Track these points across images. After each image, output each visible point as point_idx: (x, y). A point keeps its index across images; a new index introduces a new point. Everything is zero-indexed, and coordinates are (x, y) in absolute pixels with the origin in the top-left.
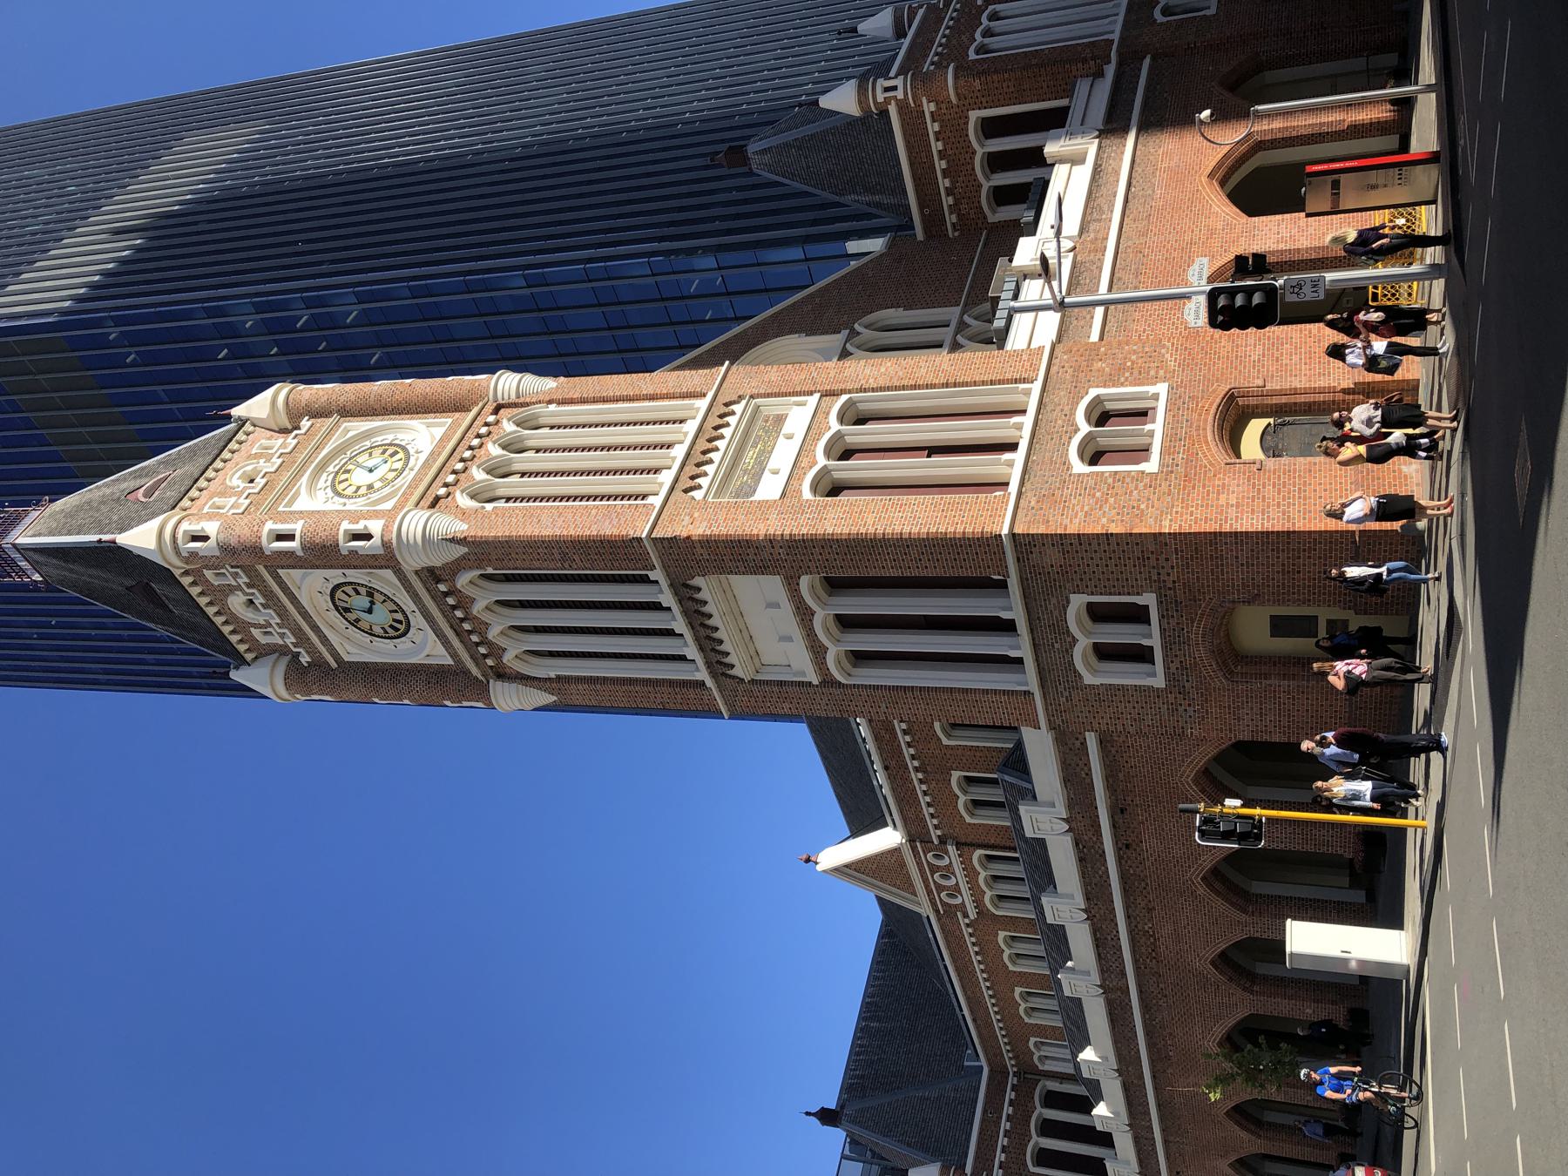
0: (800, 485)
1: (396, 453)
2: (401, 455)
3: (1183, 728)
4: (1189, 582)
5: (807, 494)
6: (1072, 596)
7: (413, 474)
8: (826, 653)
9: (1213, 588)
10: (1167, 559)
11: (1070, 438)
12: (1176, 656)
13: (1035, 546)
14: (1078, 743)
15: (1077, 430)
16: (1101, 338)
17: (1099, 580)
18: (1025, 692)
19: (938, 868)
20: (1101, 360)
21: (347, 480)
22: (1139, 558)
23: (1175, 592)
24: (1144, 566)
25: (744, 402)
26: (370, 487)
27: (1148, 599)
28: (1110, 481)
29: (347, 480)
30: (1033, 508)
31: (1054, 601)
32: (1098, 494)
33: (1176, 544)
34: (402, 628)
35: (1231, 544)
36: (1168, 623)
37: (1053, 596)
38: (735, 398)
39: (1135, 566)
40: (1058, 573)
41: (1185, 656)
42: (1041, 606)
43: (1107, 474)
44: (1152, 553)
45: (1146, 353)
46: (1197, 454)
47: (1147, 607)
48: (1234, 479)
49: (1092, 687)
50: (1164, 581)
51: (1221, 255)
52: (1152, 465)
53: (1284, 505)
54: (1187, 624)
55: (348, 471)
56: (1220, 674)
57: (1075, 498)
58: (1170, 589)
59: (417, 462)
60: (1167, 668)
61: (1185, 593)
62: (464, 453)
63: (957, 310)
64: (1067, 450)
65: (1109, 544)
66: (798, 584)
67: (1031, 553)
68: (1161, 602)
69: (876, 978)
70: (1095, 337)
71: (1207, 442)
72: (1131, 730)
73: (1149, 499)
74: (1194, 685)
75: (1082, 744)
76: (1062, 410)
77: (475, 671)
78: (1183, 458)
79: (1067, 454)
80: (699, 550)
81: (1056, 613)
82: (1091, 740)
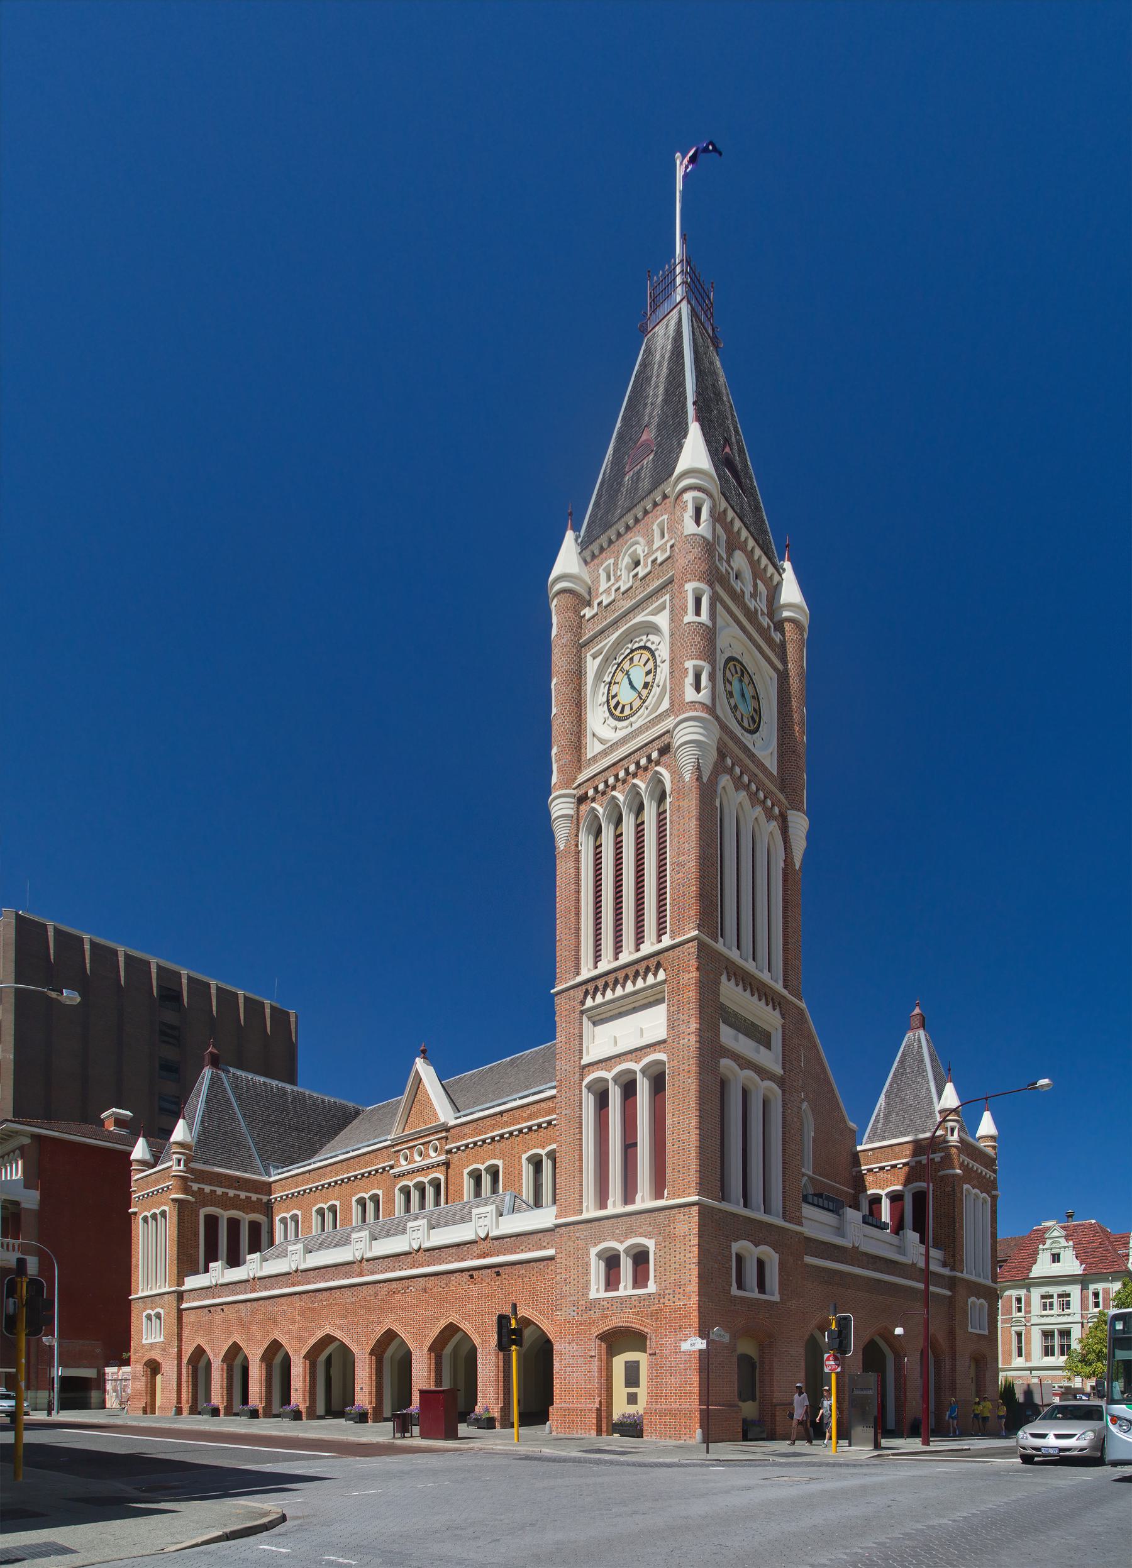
3: (561, 1310)
4: (664, 1312)
8: (607, 1071)
9: (659, 1327)
10: (679, 1299)
12: (612, 1305)
13: (689, 1217)
14: (545, 1244)
17: (665, 1258)
18: (582, 1210)
22: (680, 1282)
23: (657, 1304)
24: (675, 1286)
27: (652, 1287)
30: (712, 1217)
31: (650, 1229)
33: (690, 1304)
36: (635, 1300)
39: (675, 1280)
40: (670, 1232)
41: (612, 1310)
44: (684, 1290)
47: (646, 1286)
49: (588, 1254)
50: (664, 1298)
54: (635, 1312)
56: (601, 1331)
57: (718, 1243)
58: (659, 1301)
60: (604, 1299)
61: (656, 1310)
65: (690, 1264)
66: (659, 1052)
67: (684, 1215)
68: (650, 1296)
72: (558, 1277)
75: (545, 1247)
77: (582, 778)
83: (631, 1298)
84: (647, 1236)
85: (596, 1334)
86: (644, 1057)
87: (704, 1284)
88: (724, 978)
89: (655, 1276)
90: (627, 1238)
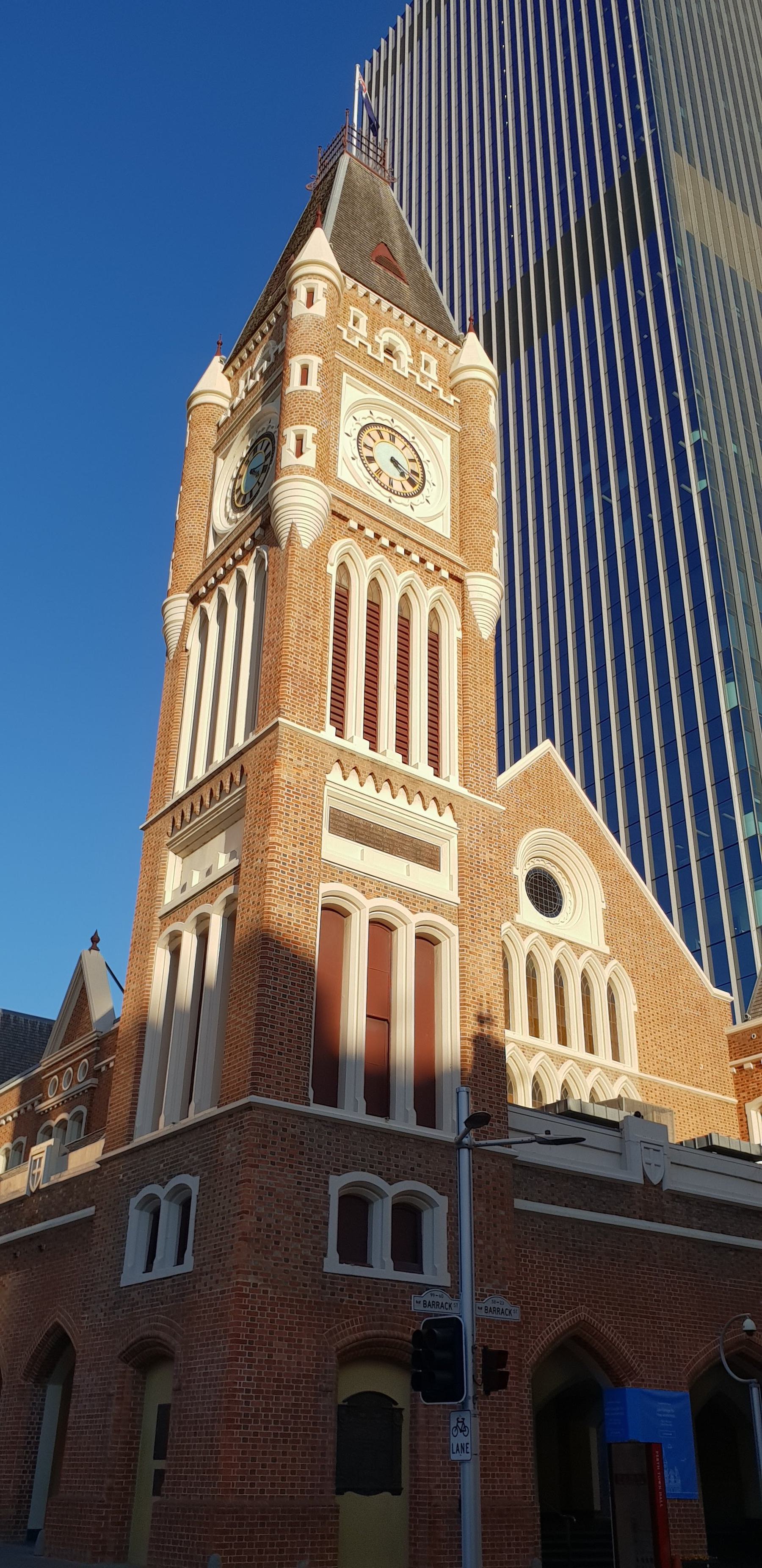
0: (340, 881)
1: (412, 482)
2: (409, 489)
5: (325, 888)
6: (198, 1178)
7: (386, 501)
11: (380, 1174)
15: (391, 1182)
19: (75, 1071)
20: (488, 1210)
21: (382, 437)
24: (214, 1257)
25: (455, 825)
26: (371, 459)
28: (317, 1217)
29: (382, 437)
30: (285, 1130)
32: (298, 1203)
34: (239, 505)
35: (223, 1354)
37: (200, 1157)
38: (459, 815)
42: (193, 1145)
43: (324, 1214)
45: (496, 1263)
46: (347, 1318)
48: (308, 1359)
51: (636, 1352)
52: (332, 1264)
53: (266, 1416)
55: (393, 439)
56: (124, 1348)
58: (194, 1287)
59: (401, 505)
62: (402, 546)
63: (635, 1070)
64: (363, 1170)
69: (34, 1025)
71: (363, 1328)
73: (287, 1260)
74: (120, 1319)
76: (419, 1165)
78: (342, 1300)
79: (357, 1170)
80: (266, 776)
81: (186, 1162)
82: (90, 1211)
83: (163, 1283)
84: (191, 1170)
85: (120, 1351)
86: (220, 894)
87: (257, 1252)
88: (335, 775)
89: (194, 1241)
90: (171, 1177)
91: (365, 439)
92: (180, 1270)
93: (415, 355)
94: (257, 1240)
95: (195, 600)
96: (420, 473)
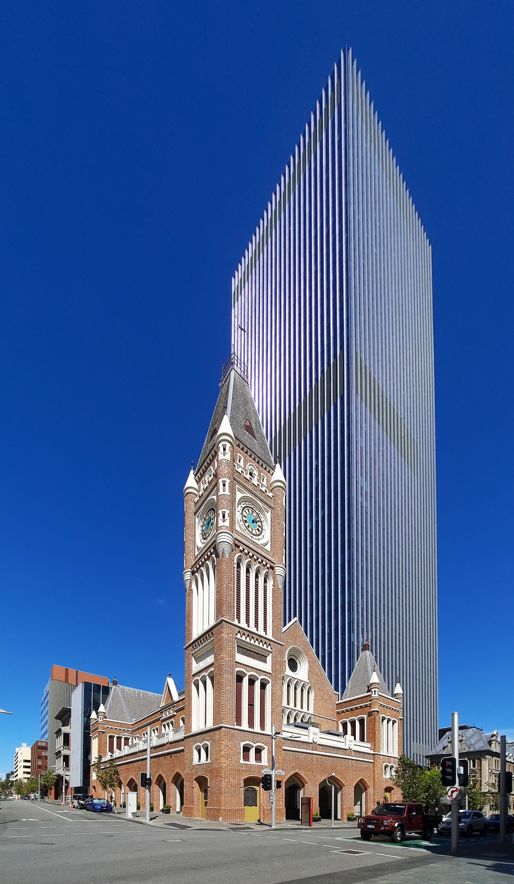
0: (241, 667)
1: (259, 531)
2: (258, 533)
5: (237, 669)
16: (284, 750)
52: (242, 761)
59: (255, 539)
62: (256, 556)
70: (284, 748)
91: (244, 513)
92: (207, 762)
93: (259, 475)
94: (225, 757)
95: (193, 573)
96: (261, 526)
